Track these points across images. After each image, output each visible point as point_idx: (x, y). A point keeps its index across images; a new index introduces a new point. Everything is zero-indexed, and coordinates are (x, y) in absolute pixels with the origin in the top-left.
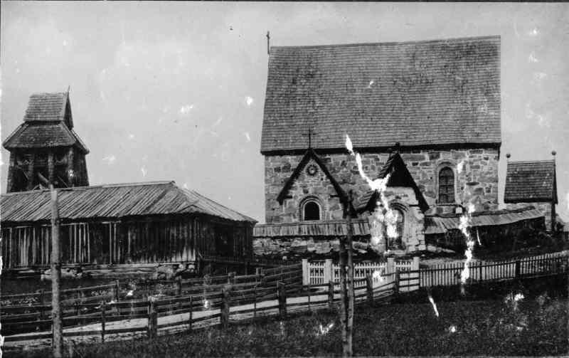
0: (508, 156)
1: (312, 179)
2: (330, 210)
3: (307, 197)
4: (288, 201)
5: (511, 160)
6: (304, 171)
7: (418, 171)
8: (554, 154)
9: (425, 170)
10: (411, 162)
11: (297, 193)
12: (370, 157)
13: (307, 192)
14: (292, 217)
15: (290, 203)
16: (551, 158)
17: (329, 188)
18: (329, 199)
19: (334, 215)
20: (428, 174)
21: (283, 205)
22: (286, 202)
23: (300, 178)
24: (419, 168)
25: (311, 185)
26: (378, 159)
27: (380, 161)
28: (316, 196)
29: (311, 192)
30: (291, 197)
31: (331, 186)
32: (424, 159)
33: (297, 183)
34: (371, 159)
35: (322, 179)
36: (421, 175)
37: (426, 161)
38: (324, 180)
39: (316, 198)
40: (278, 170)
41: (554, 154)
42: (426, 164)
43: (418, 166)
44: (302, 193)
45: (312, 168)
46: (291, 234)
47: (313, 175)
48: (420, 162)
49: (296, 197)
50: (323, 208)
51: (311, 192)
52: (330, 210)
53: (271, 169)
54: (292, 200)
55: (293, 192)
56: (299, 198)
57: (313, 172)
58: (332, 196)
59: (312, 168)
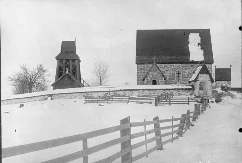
0: (215, 67)
4: (147, 79)
5: (216, 68)
8: (231, 66)
16: (230, 67)
20: (190, 72)
31: (161, 74)
36: (187, 72)
40: (141, 69)
41: (231, 66)
47: (156, 71)
48: (187, 68)
51: (154, 75)
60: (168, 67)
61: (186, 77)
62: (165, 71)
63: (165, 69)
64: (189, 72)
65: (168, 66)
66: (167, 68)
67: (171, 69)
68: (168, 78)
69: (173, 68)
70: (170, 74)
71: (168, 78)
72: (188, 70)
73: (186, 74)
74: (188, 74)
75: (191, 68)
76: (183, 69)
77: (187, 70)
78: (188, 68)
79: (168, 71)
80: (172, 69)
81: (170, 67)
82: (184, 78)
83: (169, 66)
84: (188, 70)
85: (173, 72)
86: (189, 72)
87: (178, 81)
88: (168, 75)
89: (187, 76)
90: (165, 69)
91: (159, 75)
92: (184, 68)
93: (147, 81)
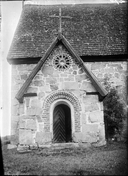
1: (63, 73)
2: (86, 111)
4: (31, 99)
13: (56, 88)
14: (37, 121)
15: (32, 101)
17: (84, 82)
19: (91, 117)
21: (25, 105)
22: (28, 101)
25: (61, 80)
28: (66, 92)
29: (61, 87)
30: (35, 95)
34: (114, 68)
38: (78, 74)
39: (67, 95)
44: (50, 90)
45: (62, 59)
46: (48, 141)
50: (76, 110)
52: (86, 111)
54: (36, 98)
56: (46, 95)
57: (62, 64)
58: (88, 94)
59: (62, 59)
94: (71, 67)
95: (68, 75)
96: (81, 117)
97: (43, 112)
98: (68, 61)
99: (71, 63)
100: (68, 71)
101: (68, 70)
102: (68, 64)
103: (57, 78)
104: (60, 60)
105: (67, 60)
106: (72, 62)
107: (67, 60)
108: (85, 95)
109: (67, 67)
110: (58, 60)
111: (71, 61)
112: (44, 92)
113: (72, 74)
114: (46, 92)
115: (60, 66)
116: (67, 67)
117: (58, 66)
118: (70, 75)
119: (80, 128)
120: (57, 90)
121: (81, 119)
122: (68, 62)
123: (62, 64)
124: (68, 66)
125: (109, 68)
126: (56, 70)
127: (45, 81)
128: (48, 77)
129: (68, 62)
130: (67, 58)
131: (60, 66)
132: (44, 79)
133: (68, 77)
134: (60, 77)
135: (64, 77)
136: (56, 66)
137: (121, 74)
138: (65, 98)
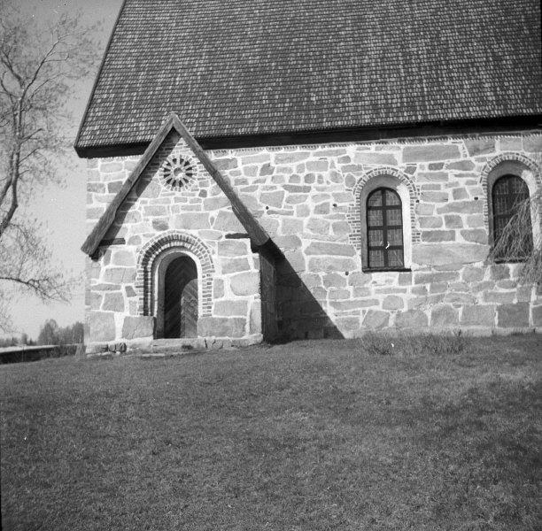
1: (178, 194)
3: (162, 242)
6: (158, 176)
7: (442, 183)
9: (462, 182)
10: (426, 164)
11: (139, 230)
12: (330, 154)
15: (117, 255)
18: (222, 246)
20: (468, 189)
23: (148, 189)
24: (445, 177)
25: (175, 210)
26: (347, 159)
27: (352, 163)
29: (173, 228)
30: (122, 241)
32: (457, 154)
33: (139, 207)
34: (329, 159)
35: (203, 194)
36: (449, 191)
37: (462, 159)
42: (463, 166)
43: (444, 170)
44: (152, 231)
48: (446, 161)
49: (134, 240)
53: (102, 186)
55: (128, 229)
56: (144, 241)
57: (180, 176)
60: (305, 161)
61: (444, 228)
62: (287, 194)
63: (287, 176)
64: (458, 193)
65: (307, 155)
66: (301, 168)
67: (326, 174)
68: (306, 244)
69: (338, 166)
70: (322, 210)
71: (306, 244)
72: (452, 179)
73: (442, 205)
74: (452, 208)
75: (473, 159)
76: (411, 170)
77: (445, 177)
78: (449, 167)
79: (307, 189)
80: (335, 177)
81: (322, 165)
82: (427, 235)
83: (312, 158)
84: (452, 179)
85: (337, 196)
86: (458, 193)
87: (386, 261)
88: (306, 220)
89: (450, 220)
90: (287, 183)
91: (214, 213)
92: (422, 166)
93: (111, 266)
94: (196, 182)
95: (189, 198)
96: (212, 285)
97: (138, 276)
98: (190, 169)
99: (195, 174)
100: (188, 191)
101: (189, 188)
102: (190, 175)
103: (166, 206)
104: (172, 169)
105: (187, 167)
106: (199, 169)
107: (187, 167)
108: (224, 239)
109: (187, 181)
110: (169, 168)
111: (196, 170)
112: (141, 235)
113: (197, 196)
114: (144, 235)
115: (172, 182)
116: (187, 181)
117: (168, 182)
118: (192, 198)
119: (210, 307)
120: (166, 231)
121: (213, 289)
122: (189, 172)
123: (180, 176)
124: (190, 179)
125: (317, 159)
126: (165, 188)
127: (142, 212)
128: (148, 205)
129: (189, 172)
130: (187, 163)
131: (172, 182)
132: (140, 208)
133: (188, 203)
134: (173, 203)
135: (180, 204)
136: (166, 180)
137: (346, 174)
138: (183, 247)
